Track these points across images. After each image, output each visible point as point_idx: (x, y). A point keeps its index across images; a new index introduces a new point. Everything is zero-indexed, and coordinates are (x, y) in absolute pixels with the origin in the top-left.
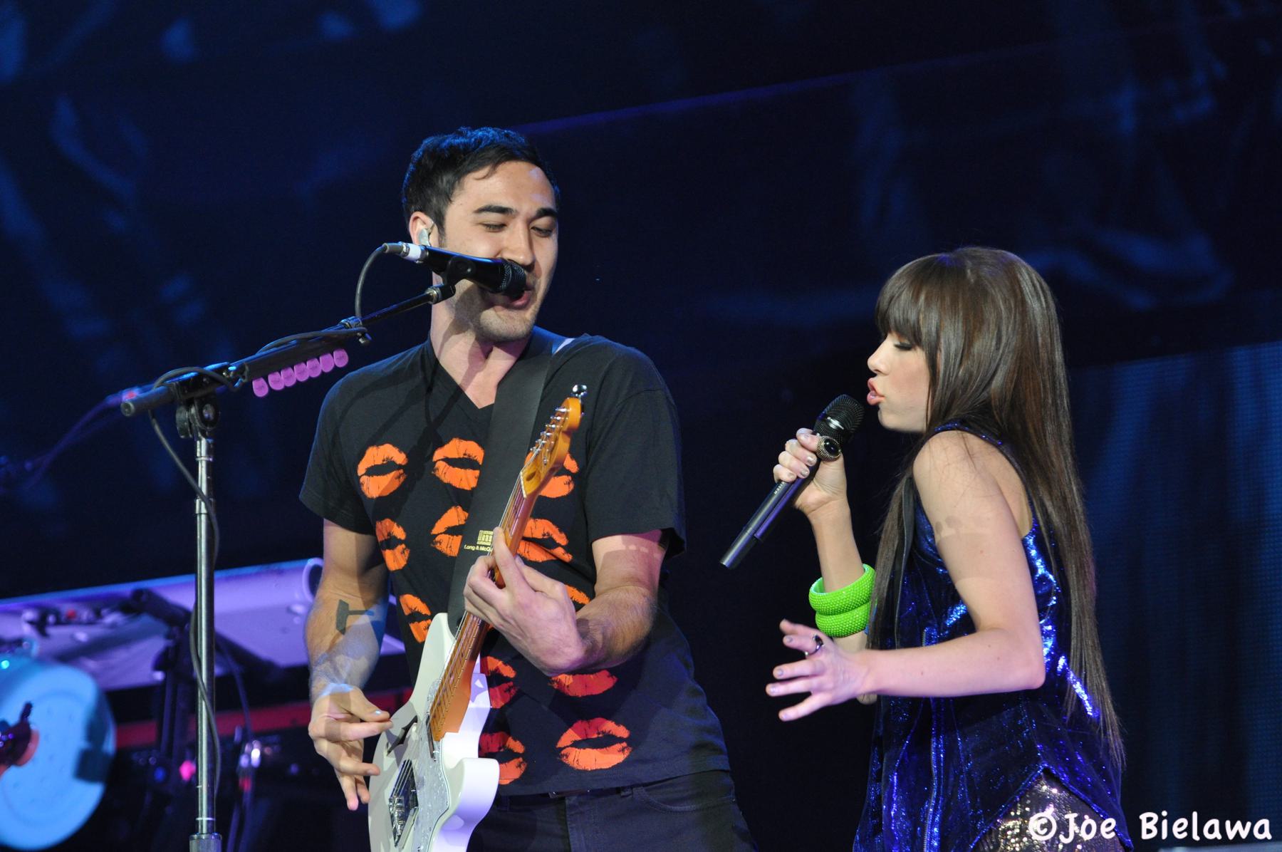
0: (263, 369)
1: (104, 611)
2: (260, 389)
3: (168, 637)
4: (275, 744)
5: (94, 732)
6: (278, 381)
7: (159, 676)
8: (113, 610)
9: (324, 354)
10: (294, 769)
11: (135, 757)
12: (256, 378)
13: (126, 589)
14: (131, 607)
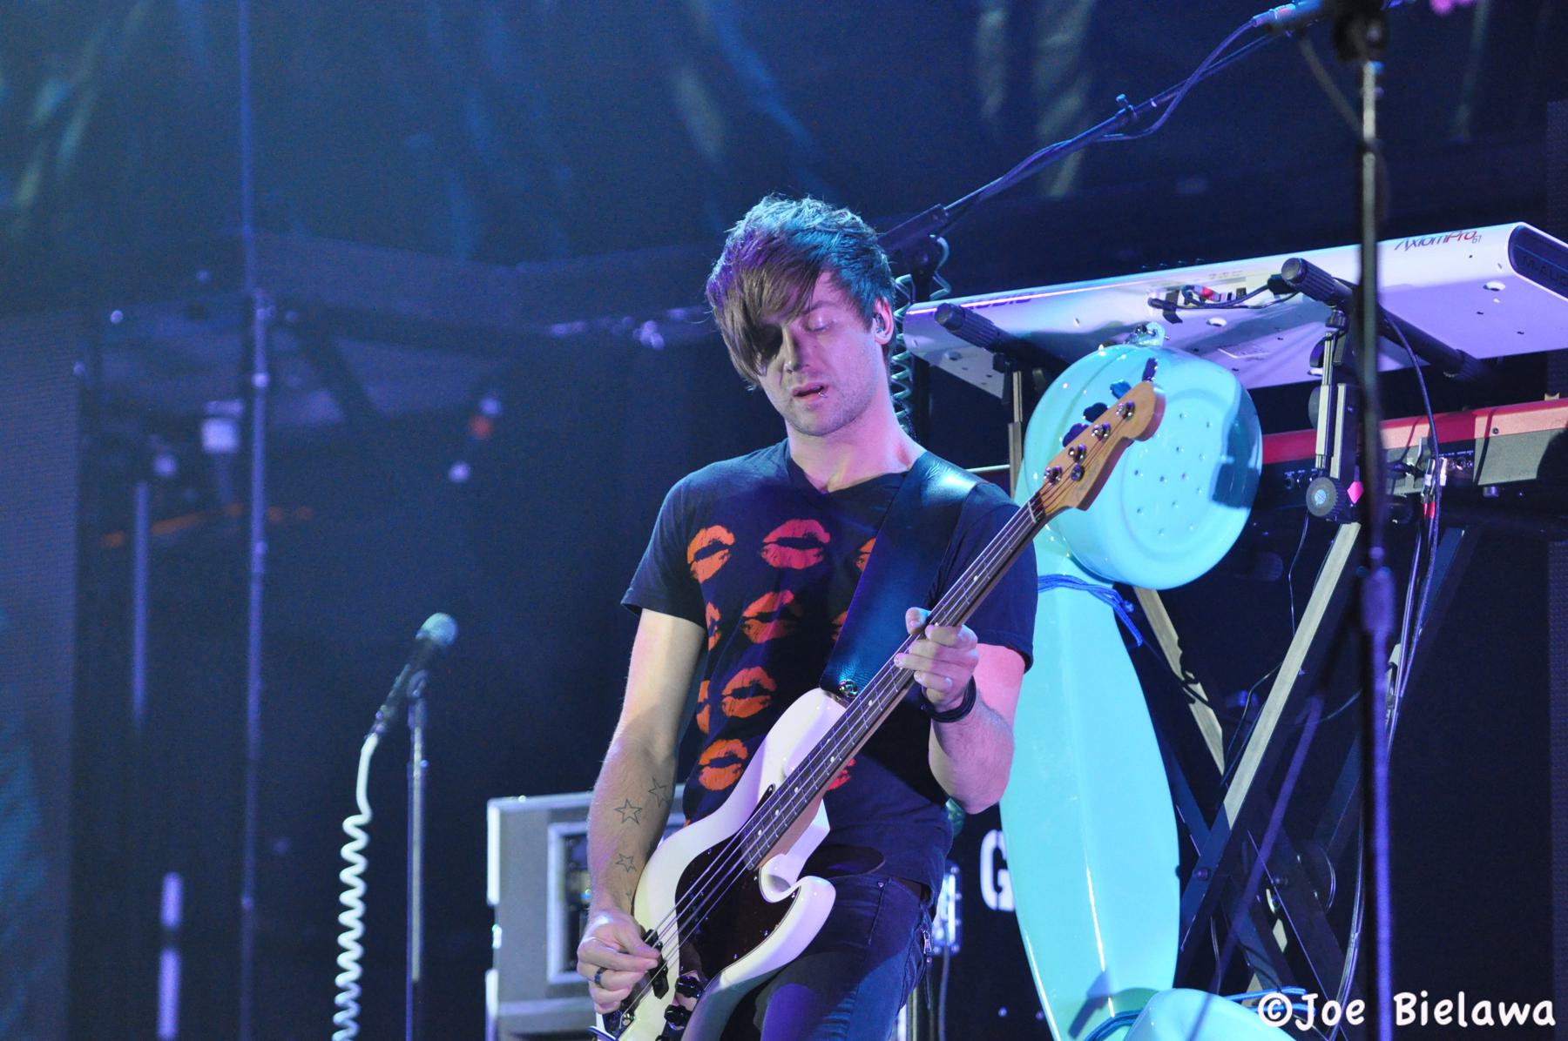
11: (1289, 474)
13: (1273, 265)
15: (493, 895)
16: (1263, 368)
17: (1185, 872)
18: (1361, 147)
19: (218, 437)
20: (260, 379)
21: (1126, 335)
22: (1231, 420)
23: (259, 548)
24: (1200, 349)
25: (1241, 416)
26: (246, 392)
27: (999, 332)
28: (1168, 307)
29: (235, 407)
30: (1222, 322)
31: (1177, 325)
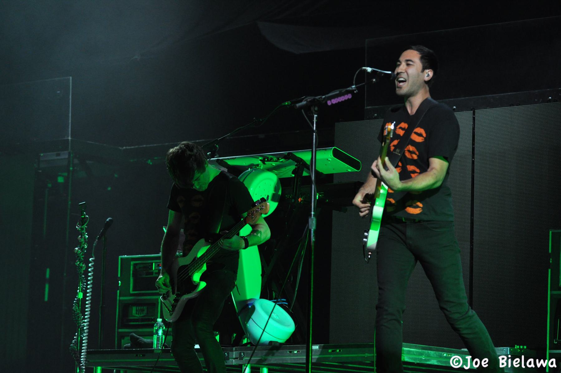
0: (331, 98)
1: (280, 159)
2: (329, 103)
3: (296, 165)
4: (322, 194)
5: (276, 189)
6: (333, 101)
7: (293, 175)
8: (282, 158)
9: (345, 95)
10: (327, 200)
11: (286, 196)
12: (329, 100)
14: (286, 157)
15: (119, 275)
16: (281, 174)
17: (263, 275)
18: (313, 131)
19: (60, 180)
20: (71, 169)
21: (254, 167)
22: (275, 184)
23: (70, 203)
24: (270, 170)
25: (277, 183)
26: (68, 171)
27: (229, 165)
28: (263, 161)
29: (66, 174)
30: (274, 164)
31: (265, 165)
